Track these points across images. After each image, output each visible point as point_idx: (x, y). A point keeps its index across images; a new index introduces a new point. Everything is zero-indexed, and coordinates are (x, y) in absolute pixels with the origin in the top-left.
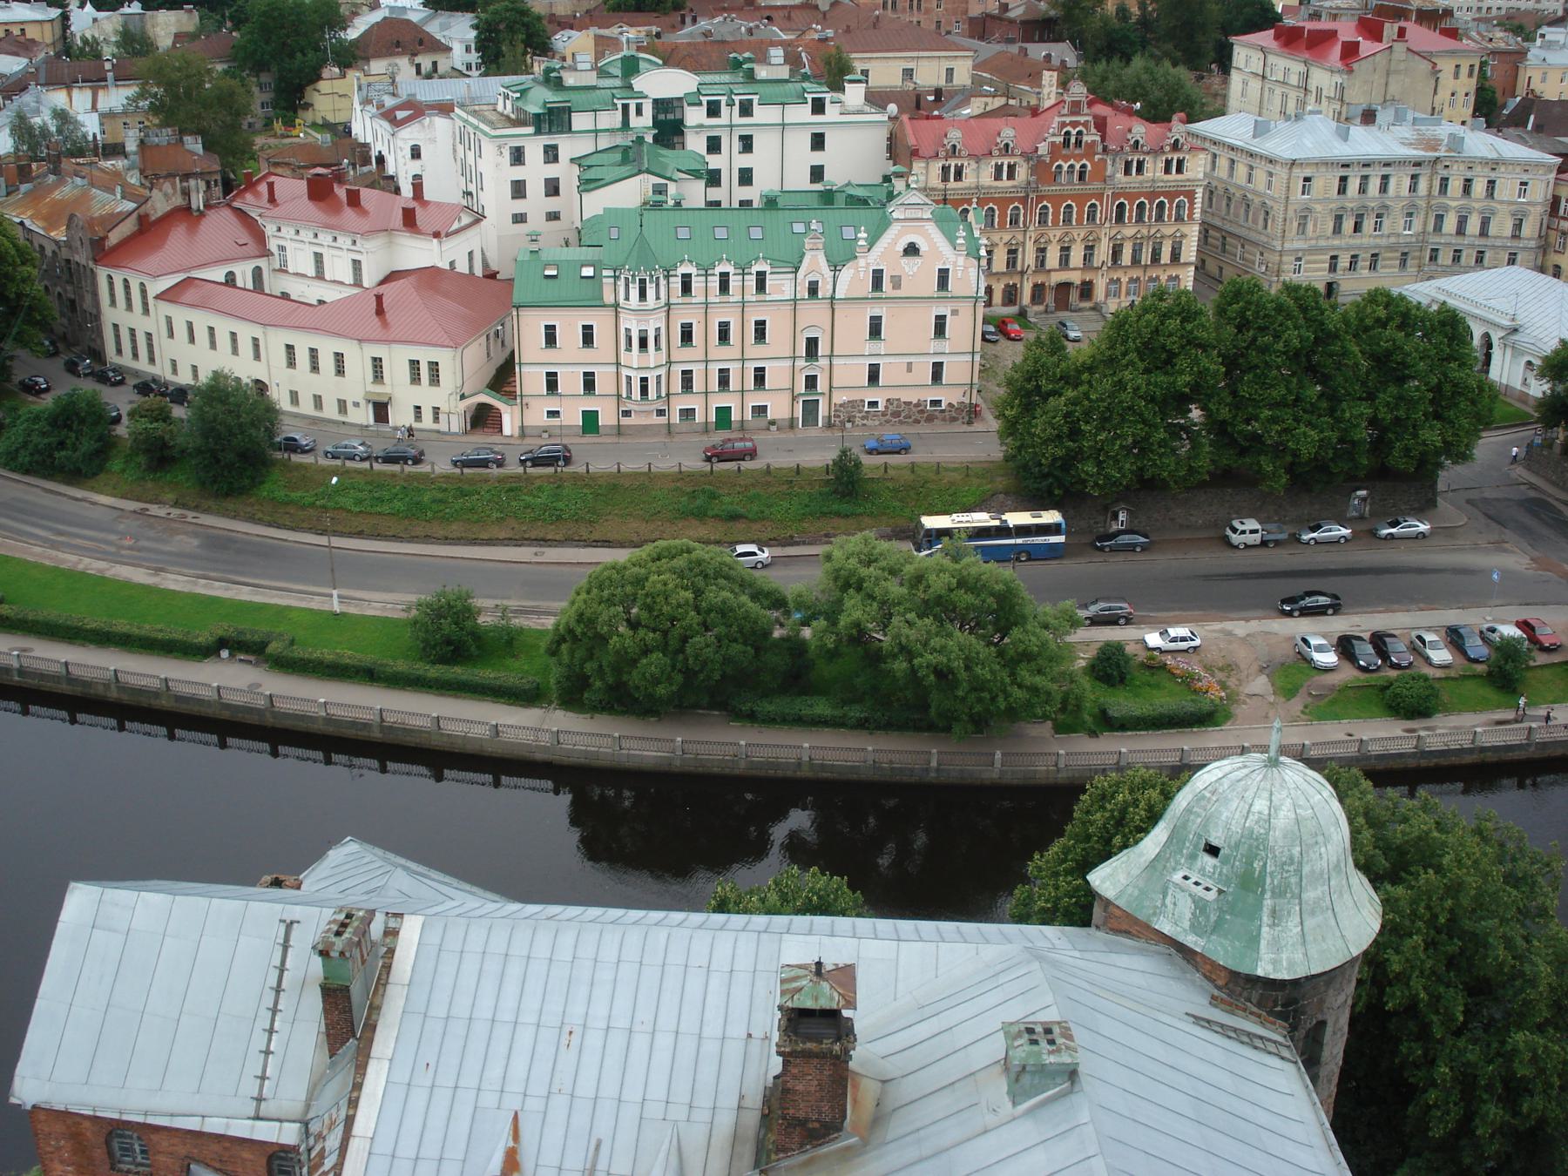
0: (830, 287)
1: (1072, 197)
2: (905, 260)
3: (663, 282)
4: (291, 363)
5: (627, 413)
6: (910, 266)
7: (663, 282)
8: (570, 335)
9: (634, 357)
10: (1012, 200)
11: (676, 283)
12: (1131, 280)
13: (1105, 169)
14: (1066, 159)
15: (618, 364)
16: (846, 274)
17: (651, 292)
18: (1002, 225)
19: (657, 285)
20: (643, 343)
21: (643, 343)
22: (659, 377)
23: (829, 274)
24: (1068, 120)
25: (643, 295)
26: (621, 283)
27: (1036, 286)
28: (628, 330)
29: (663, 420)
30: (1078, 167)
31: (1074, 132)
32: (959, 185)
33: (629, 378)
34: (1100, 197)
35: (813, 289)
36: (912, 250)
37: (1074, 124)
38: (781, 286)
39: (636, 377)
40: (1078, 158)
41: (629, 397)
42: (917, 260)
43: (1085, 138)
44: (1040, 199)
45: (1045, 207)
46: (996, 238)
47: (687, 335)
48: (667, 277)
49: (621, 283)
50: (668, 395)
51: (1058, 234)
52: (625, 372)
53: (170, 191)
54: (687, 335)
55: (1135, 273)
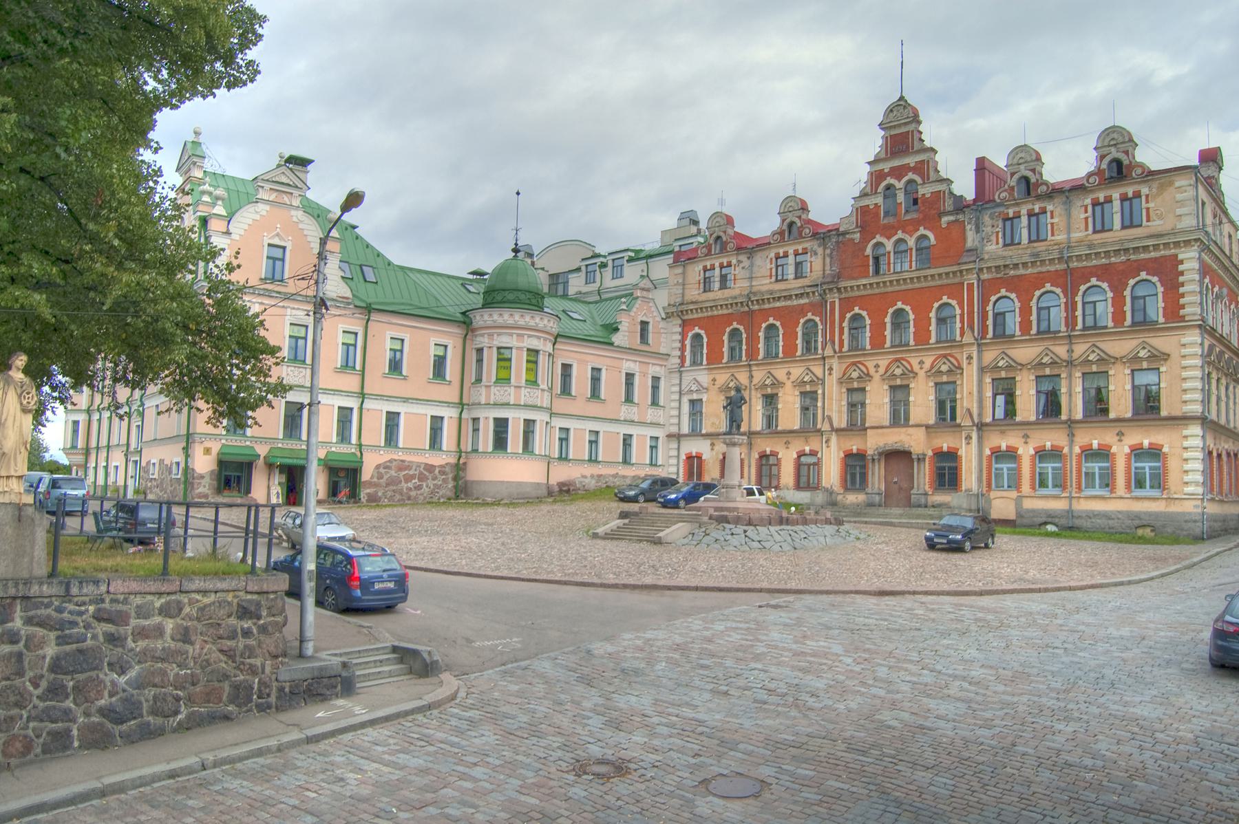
1: (905, 296)
10: (802, 310)
12: (1042, 454)
13: (964, 239)
14: (889, 231)
18: (790, 351)
24: (886, 167)
27: (849, 456)
30: (911, 242)
31: (899, 185)
32: (727, 293)
34: (955, 290)
37: (898, 172)
40: (909, 227)
43: (921, 191)
44: (847, 304)
45: (857, 317)
46: (780, 373)
51: (883, 363)
55: (1051, 438)
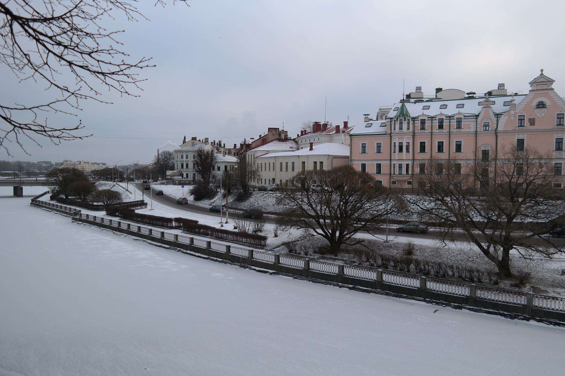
0: (495, 125)
2: (537, 110)
3: (411, 122)
4: (281, 170)
5: (394, 182)
6: (539, 114)
7: (411, 122)
8: (371, 149)
9: (396, 155)
11: (418, 124)
15: (391, 160)
16: (503, 119)
17: (405, 126)
19: (409, 123)
20: (401, 150)
21: (401, 150)
22: (407, 165)
23: (494, 119)
25: (401, 128)
26: (393, 123)
28: (395, 143)
29: (410, 186)
33: (394, 164)
35: (486, 125)
36: (541, 105)
38: (469, 126)
39: (397, 163)
41: (394, 174)
42: (544, 110)
47: (423, 149)
48: (414, 121)
49: (393, 123)
50: (413, 174)
52: (393, 162)
53: (274, 133)
54: (423, 149)
